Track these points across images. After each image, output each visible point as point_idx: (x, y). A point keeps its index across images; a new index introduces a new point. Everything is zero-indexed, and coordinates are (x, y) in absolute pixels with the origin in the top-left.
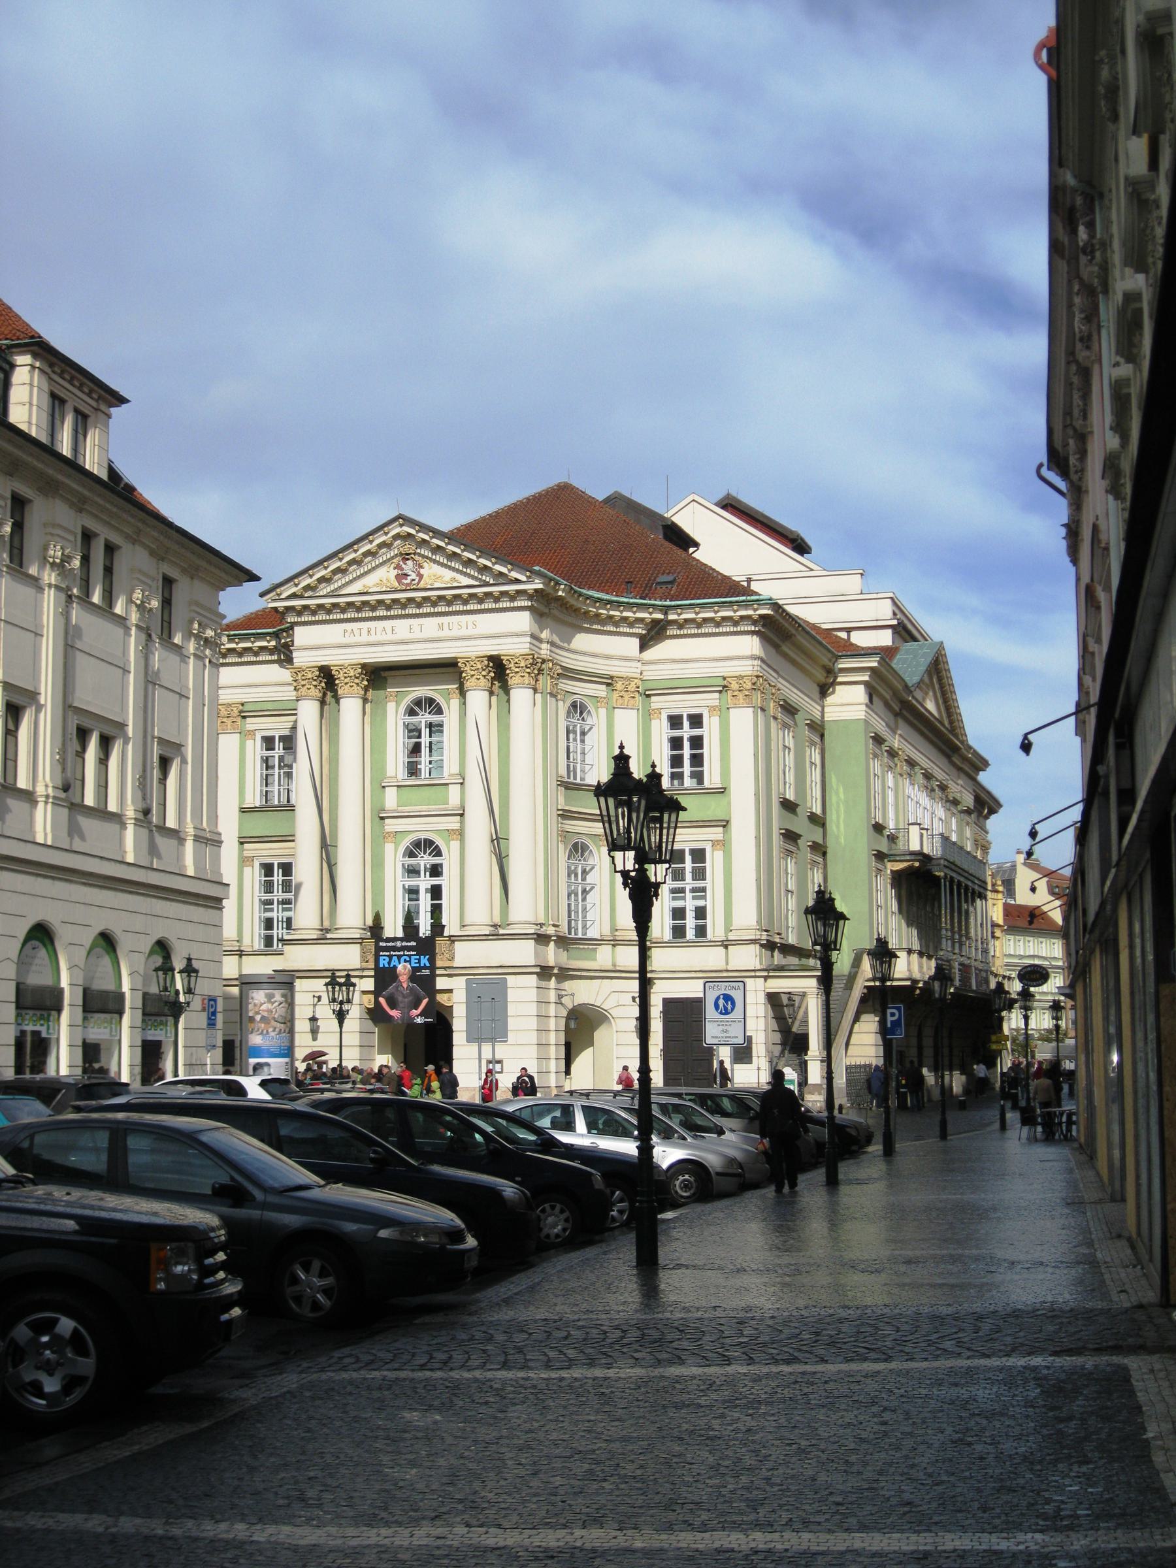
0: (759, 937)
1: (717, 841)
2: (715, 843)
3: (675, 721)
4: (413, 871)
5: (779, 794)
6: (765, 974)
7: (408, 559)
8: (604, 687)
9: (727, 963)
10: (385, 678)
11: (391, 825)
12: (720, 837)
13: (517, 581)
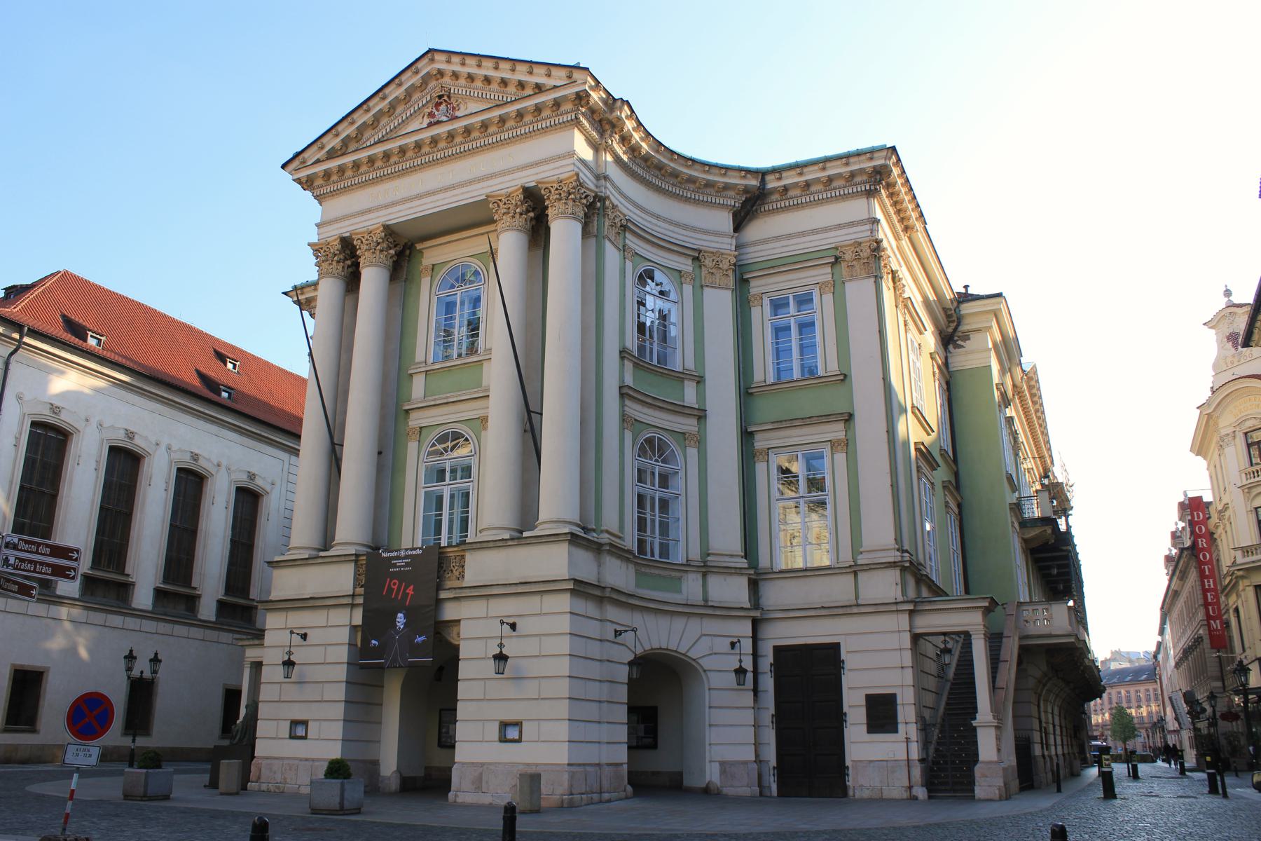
0: (899, 559)
1: (838, 440)
2: (834, 444)
3: (778, 305)
4: (440, 475)
5: (913, 404)
6: (911, 607)
7: (441, 103)
8: (690, 262)
9: (857, 598)
10: (421, 252)
11: (416, 420)
12: (841, 435)
13: (555, 87)
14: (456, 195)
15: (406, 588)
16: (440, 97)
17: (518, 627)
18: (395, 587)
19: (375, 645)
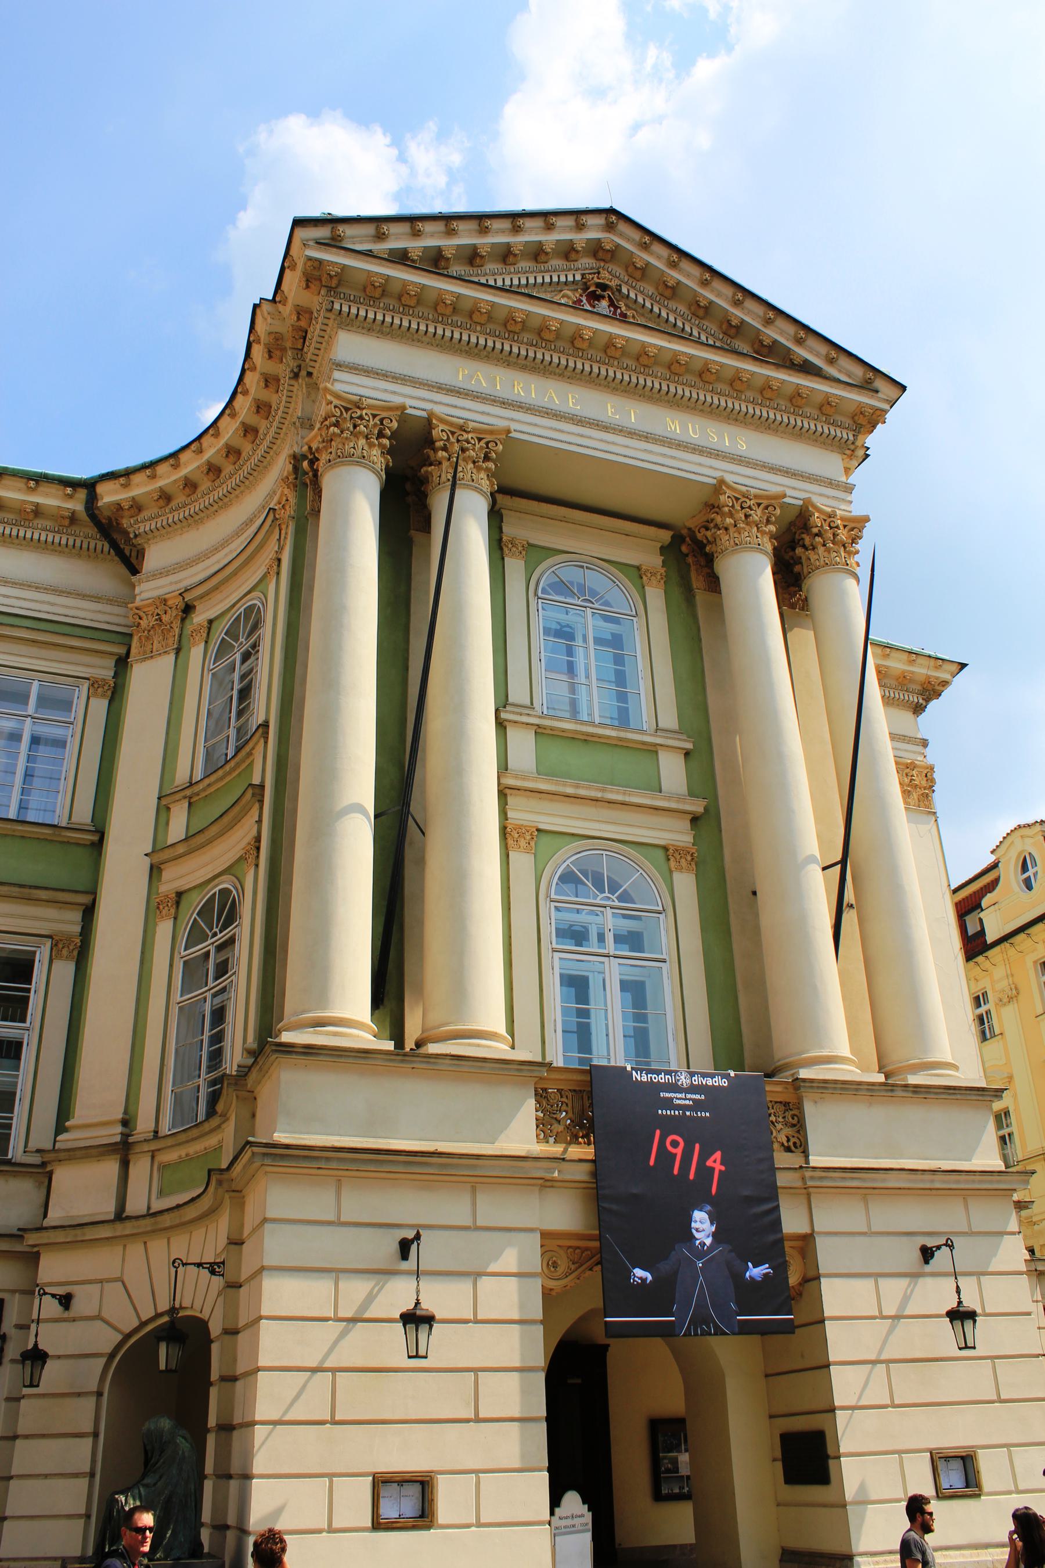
7: (603, 297)
14: (651, 452)
15: (704, 1156)
16: (604, 287)
17: (917, 1254)
18: (679, 1151)
19: (644, 1280)
